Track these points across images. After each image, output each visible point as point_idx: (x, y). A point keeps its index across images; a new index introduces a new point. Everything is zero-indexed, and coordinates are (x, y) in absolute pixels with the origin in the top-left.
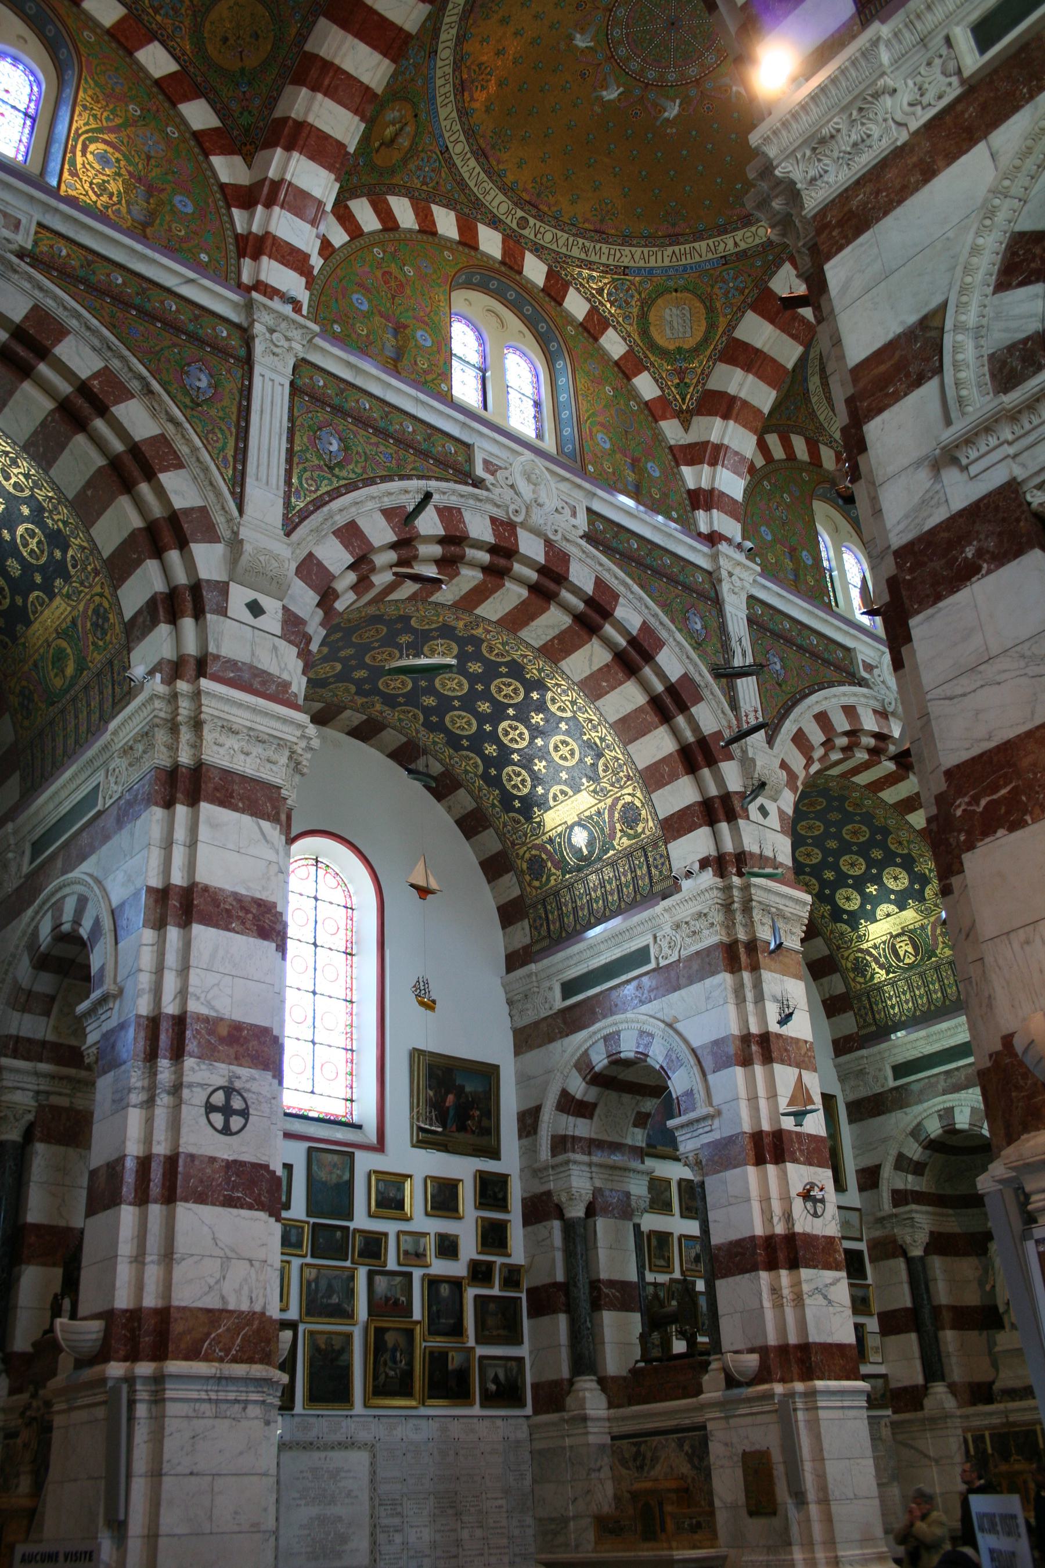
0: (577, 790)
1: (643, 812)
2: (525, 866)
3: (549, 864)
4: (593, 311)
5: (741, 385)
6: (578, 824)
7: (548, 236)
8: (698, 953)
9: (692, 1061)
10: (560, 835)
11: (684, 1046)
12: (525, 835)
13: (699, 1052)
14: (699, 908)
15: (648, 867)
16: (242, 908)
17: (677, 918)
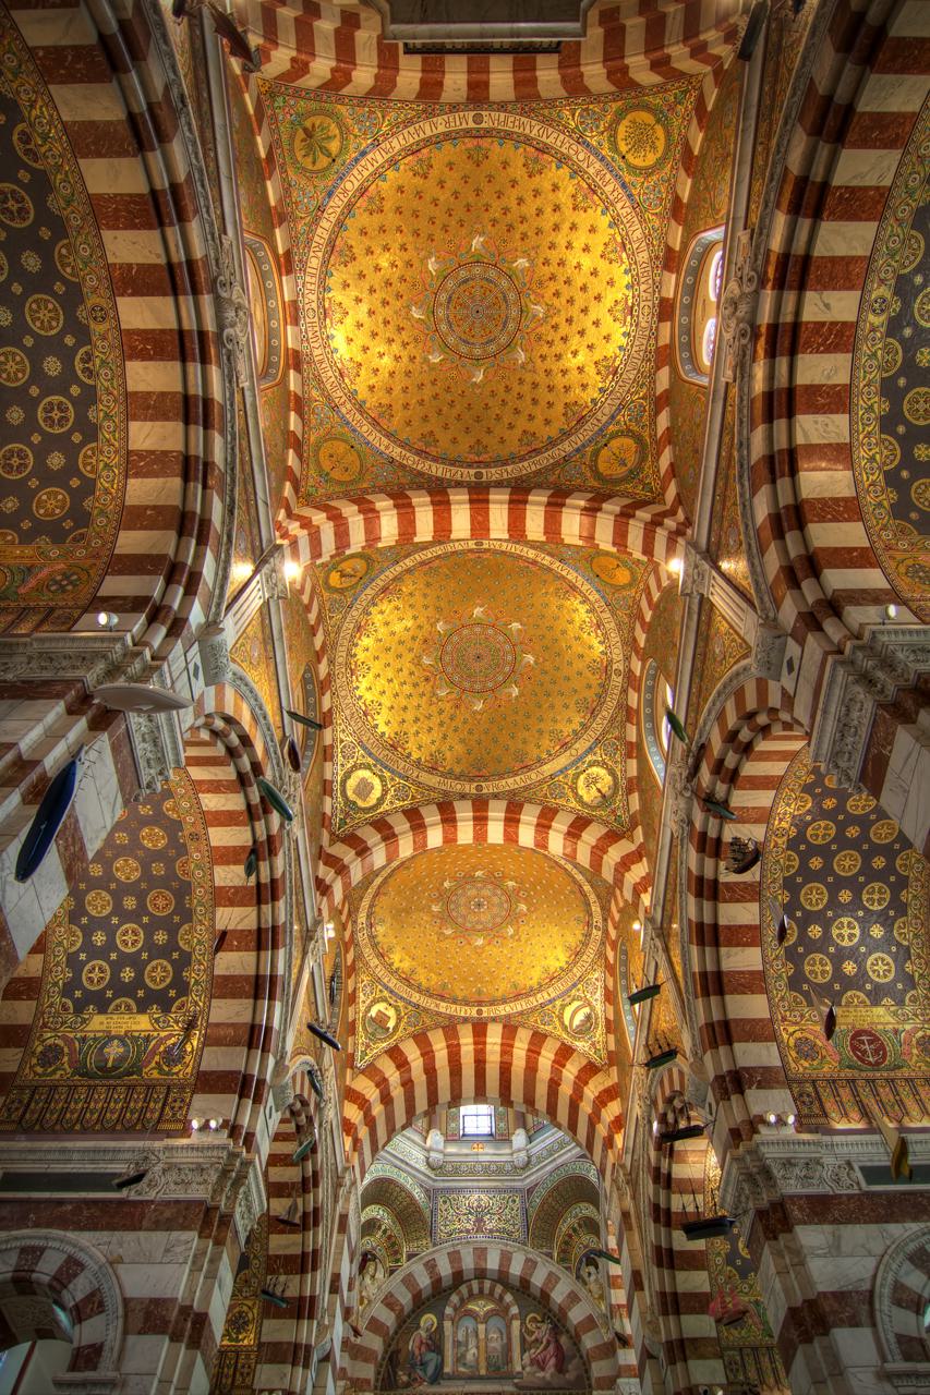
0: (142, 1009)
1: (187, 1059)
2: (40, 1049)
3: (66, 1059)
4: (332, 746)
5: (375, 845)
6: (121, 1039)
7: (343, 693)
8: (177, 1202)
9: (121, 1312)
10: (95, 1039)
11: (118, 1291)
12: (62, 1024)
13: (132, 1304)
14: (201, 1160)
15: (164, 1105)
16: (73, 838)
17: (174, 1160)
